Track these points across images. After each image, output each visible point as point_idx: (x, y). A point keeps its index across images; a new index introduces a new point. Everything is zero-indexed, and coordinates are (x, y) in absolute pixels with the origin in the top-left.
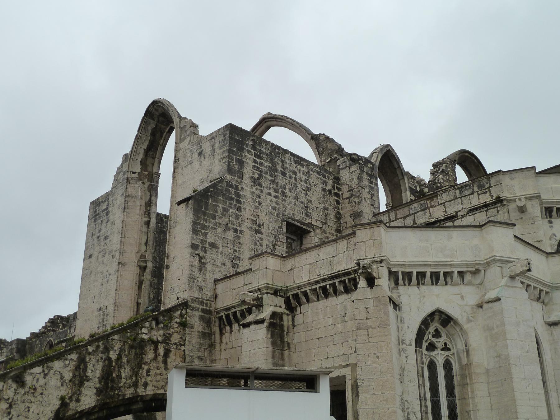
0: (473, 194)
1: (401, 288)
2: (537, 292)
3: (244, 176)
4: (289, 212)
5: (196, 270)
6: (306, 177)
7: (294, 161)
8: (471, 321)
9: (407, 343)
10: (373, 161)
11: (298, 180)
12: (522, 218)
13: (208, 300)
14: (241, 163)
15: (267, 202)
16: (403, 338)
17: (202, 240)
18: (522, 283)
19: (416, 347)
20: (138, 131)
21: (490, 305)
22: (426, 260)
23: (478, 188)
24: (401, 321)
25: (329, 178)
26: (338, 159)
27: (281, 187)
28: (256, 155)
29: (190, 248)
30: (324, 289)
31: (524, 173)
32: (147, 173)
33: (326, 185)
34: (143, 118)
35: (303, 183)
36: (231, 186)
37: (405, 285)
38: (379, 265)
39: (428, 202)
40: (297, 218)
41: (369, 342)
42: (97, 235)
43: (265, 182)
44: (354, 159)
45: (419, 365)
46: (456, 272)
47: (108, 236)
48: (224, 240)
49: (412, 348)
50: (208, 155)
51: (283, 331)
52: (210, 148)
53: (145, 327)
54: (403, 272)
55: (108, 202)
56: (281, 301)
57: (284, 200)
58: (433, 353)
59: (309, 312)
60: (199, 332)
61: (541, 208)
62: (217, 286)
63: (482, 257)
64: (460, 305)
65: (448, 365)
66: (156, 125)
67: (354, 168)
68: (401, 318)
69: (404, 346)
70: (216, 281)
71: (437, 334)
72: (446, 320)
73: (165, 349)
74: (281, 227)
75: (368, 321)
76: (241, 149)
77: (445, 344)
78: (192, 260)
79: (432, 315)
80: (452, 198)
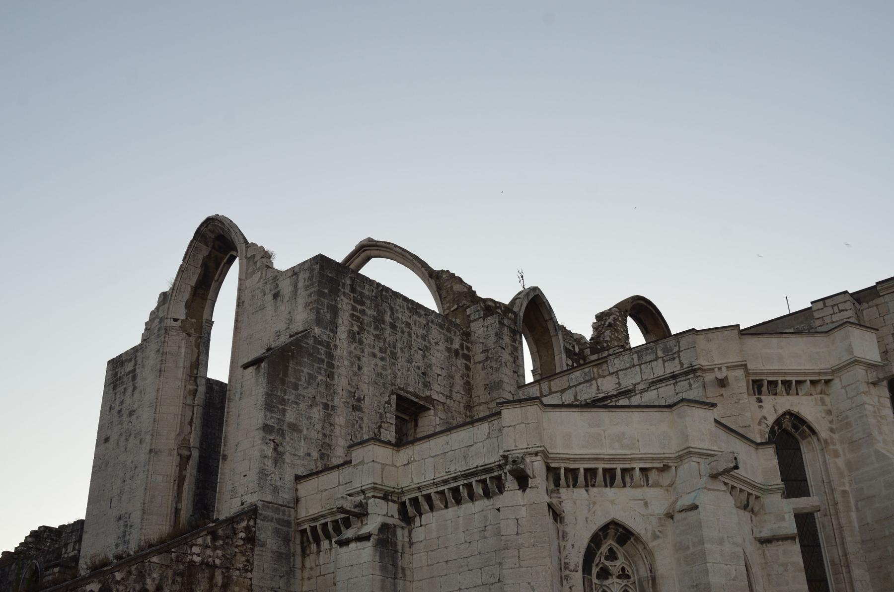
0: (656, 359)
1: (563, 491)
2: (744, 497)
3: (339, 329)
4: (400, 382)
5: (269, 462)
6: (424, 332)
7: (408, 308)
8: (658, 537)
9: (572, 567)
10: (516, 309)
13: (286, 506)
14: (335, 311)
15: (369, 367)
19: (583, 573)
20: (184, 260)
21: (683, 515)
23: (664, 353)
24: (563, 537)
25: (455, 332)
26: (469, 307)
27: (389, 345)
28: (355, 300)
29: (261, 432)
30: (455, 491)
31: (725, 333)
32: (194, 320)
33: (452, 344)
34: (192, 241)
35: (420, 340)
36: (320, 343)
37: (568, 486)
38: (534, 458)
39: (595, 370)
40: (411, 390)
41: (520, 567)
42: (117, 408)
43: (368, 338)
44: (490, 307)
46: (638, 469)
49: (579, 574)
50: (286, 299)
51: (396, 552)
52: (291, 288)
53: (196, 545)
54: (565, 469)
55: (136, 362)
56: (394, 508)
57: (394, 364)
58: (606, 582)
59: (433, 525)
60: (272, 552)
61: (748, 382)
62: (299, 487)
63: (673, 448)
66: (210, 252)
67: (490, 320)
68: (563, 532)
69: (567, 572)
70: (298, 478)
73: (224, 577)
74: (388, 402)
76: (334, 292)
77: (623, 569)
78: (265, 448)
79: (605, 528)
80: (628, 365)
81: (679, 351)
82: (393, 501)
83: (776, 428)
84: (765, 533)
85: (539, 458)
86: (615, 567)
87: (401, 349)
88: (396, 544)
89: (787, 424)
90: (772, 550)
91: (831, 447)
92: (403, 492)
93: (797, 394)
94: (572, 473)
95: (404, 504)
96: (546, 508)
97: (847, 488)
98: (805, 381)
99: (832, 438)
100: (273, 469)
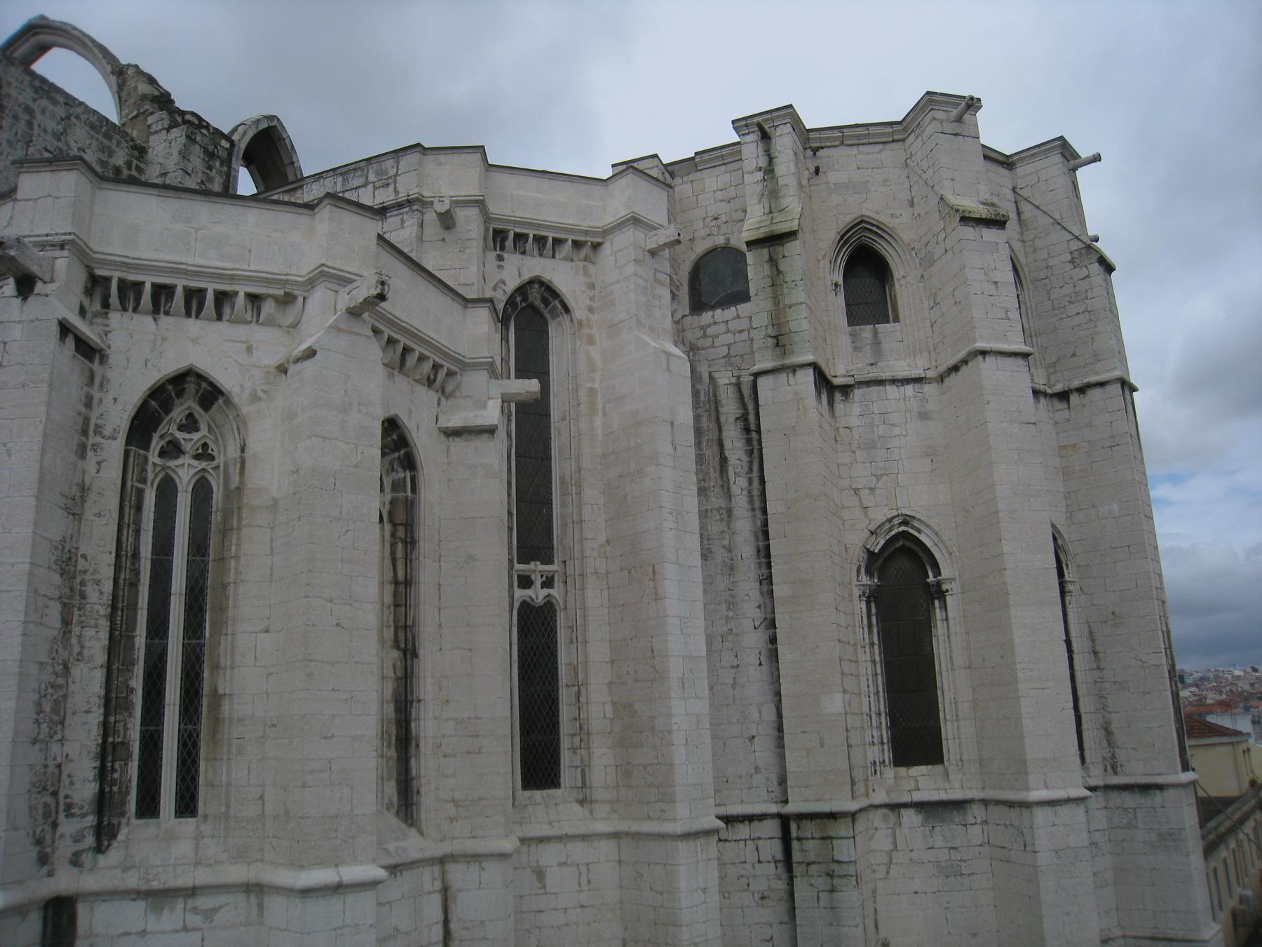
0: (364, 186)
6: (60, 128)
7: (32, 86)
8: (260, 399)
9: (107, 432)
10: (235, 137)
11: (36, 126)
12: (443, 240)
16: (99, 421)
18: (376, 331)
19: (128, 442)
21: (299, 366)
22: (178, 259)
24: (101, 385)
25: (119, 144)
26: (152, 113)
31: (463, 156)
33: (110, 156)
35: (49, 138)
37: (125, 309)
38: (58, 253)
45: (129, 484)
46: (241, 295)
58: (172, 463)
61: (487, 230)
63: (303, 269)
65: (202, 490)
67: (175, 132)
68: (103, 378)
69: (98, 439)
71: (190, 424)
72: (211, 394)
77: (205, 445)
81: (396, 175)
83: (518, 299)
84: (455, 422)
85: (65, 253)
86: (190, 441)
87: (9, 142)
89: (535, 295)
90: (458, 445)
91: (586, 330)
93: (554, 257)
94: (130, 291)
96: (55, 329)
97: (597, 385)
98: (566, 240)
99: (588, 319)
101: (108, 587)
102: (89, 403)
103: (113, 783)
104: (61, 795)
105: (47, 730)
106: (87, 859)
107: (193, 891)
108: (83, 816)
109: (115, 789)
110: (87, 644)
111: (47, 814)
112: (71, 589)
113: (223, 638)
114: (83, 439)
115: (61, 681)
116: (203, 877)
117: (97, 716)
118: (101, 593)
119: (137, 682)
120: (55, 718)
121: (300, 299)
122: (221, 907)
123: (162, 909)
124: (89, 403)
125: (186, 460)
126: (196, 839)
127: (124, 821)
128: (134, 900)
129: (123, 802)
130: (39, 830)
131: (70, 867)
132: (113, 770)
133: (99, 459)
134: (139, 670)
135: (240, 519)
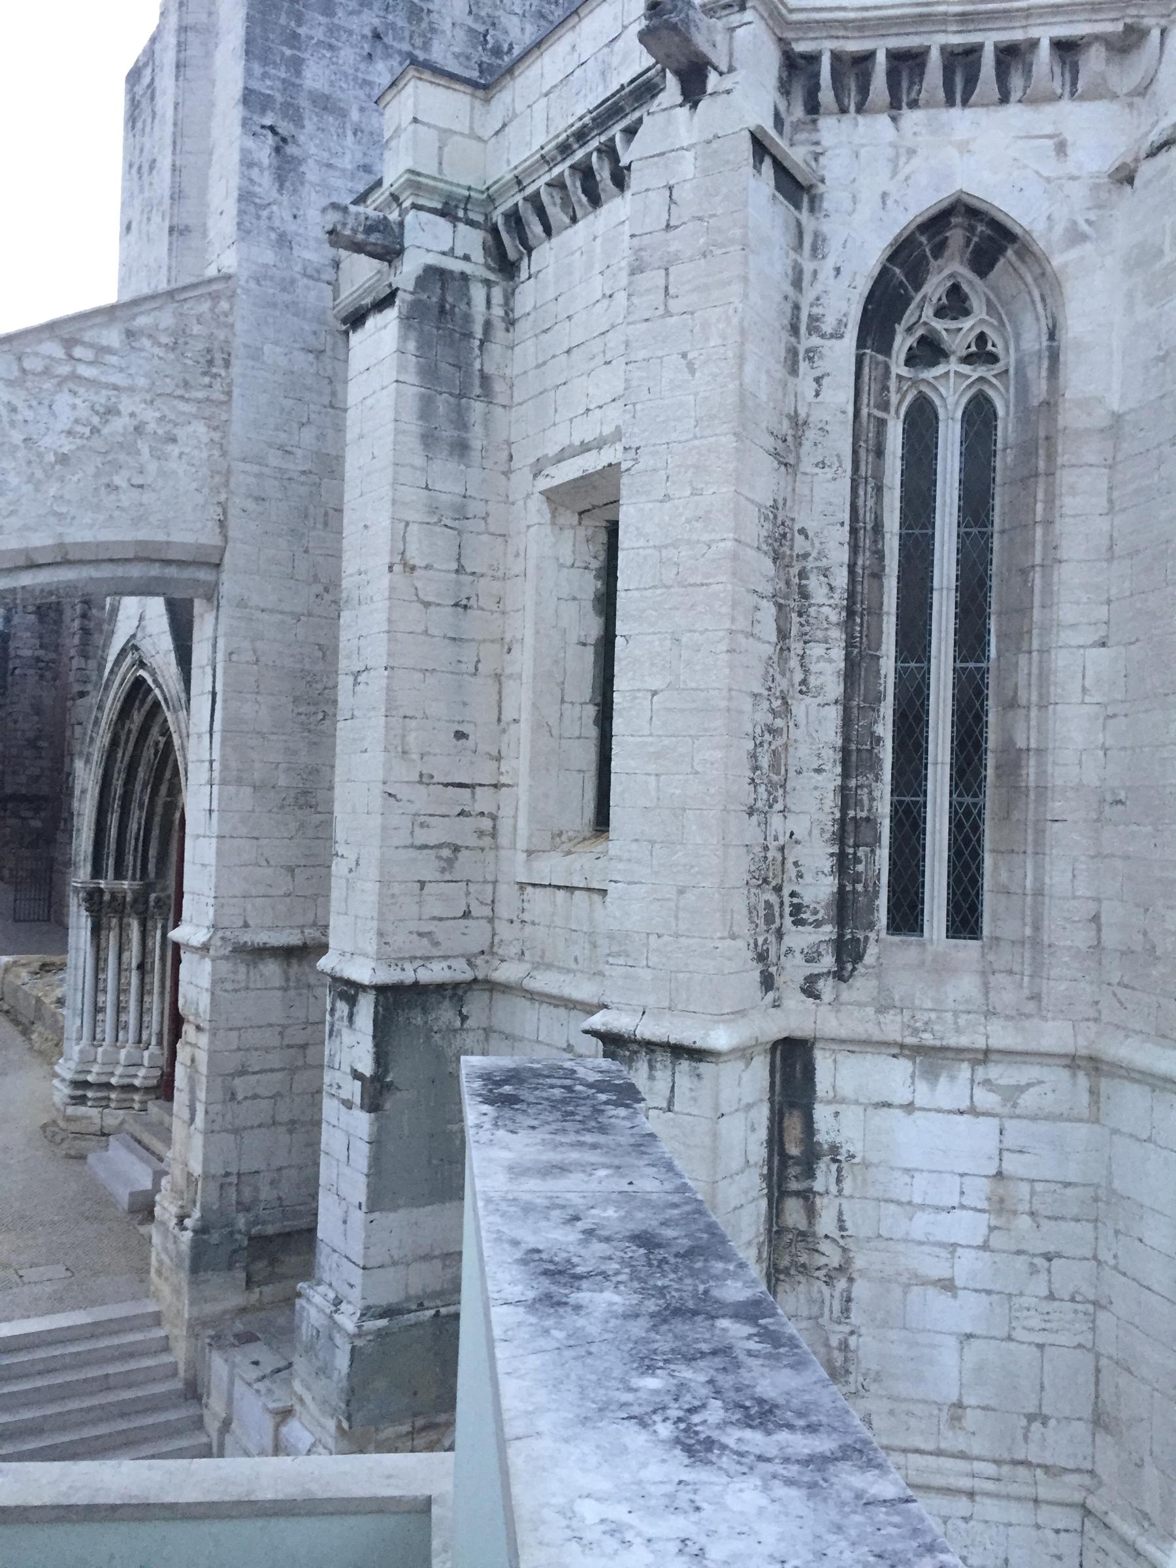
1: (827, 124)
9: (828, 326)
16: (815, 310)
17: (284, 81)
19: (861, 343)
24: (814, 249)
29: (241, 107)
30: (586, 173)
37: (843, 110)
38: (736, 19)
41: (668, 313)
45: (864, 411)
47: (154, 161)
48: (367, 89)
51: (469, 335)
53: (83, 344)
54: (836, 57)
56: (472, 241)
58: (930, 374)
59: (550, 270)
64: (1048, 180)
65: (979, 415)
68: (816, 235)
69: (815, 341)
71: (955, 303)
75: (673, 233)
77: (982, 339)
78: (250, 143)
79: (936, 224)
82: (471, 223)
85: (749, 15)
86: (958, 335)
88: (467, 318)
92: (491, 199)
95: (494, 231)
96: (746, 147)
100: (274, 194)
101: (841, 579)
102: (797, 283)
103: (856, 879)
104: (786, 892)
105: (765, 796)
106: (826, 987)
107: (985, 1056)
108: (818, 924)
109: (860, 887)
110: (813, 668)
111: (769, 919)
112: (788, 583)
113: (1023, 659)
114: (793, 339)
115: (779, 723)
116: (1001, 1036)
117: (831, 779)
118: (831, 588)
119: (885, 730)
120: (775, 778)
121: (1155, 34)
122: (1029, 1085)
123: (937, 1077)
124: (797, 283)
125: (953, 365)
126: (983, 973)
127: (872, 936)
128: (894, 1056)
129: (871, 909)
130: (760, 941)
131: (803, 997)
132: (857, 860)
133: (818, 373)
134: (887, 709)
135: (1051, 457)
